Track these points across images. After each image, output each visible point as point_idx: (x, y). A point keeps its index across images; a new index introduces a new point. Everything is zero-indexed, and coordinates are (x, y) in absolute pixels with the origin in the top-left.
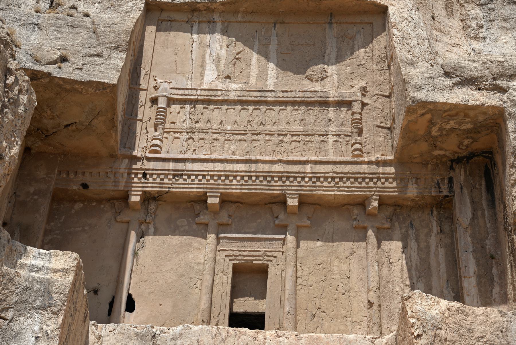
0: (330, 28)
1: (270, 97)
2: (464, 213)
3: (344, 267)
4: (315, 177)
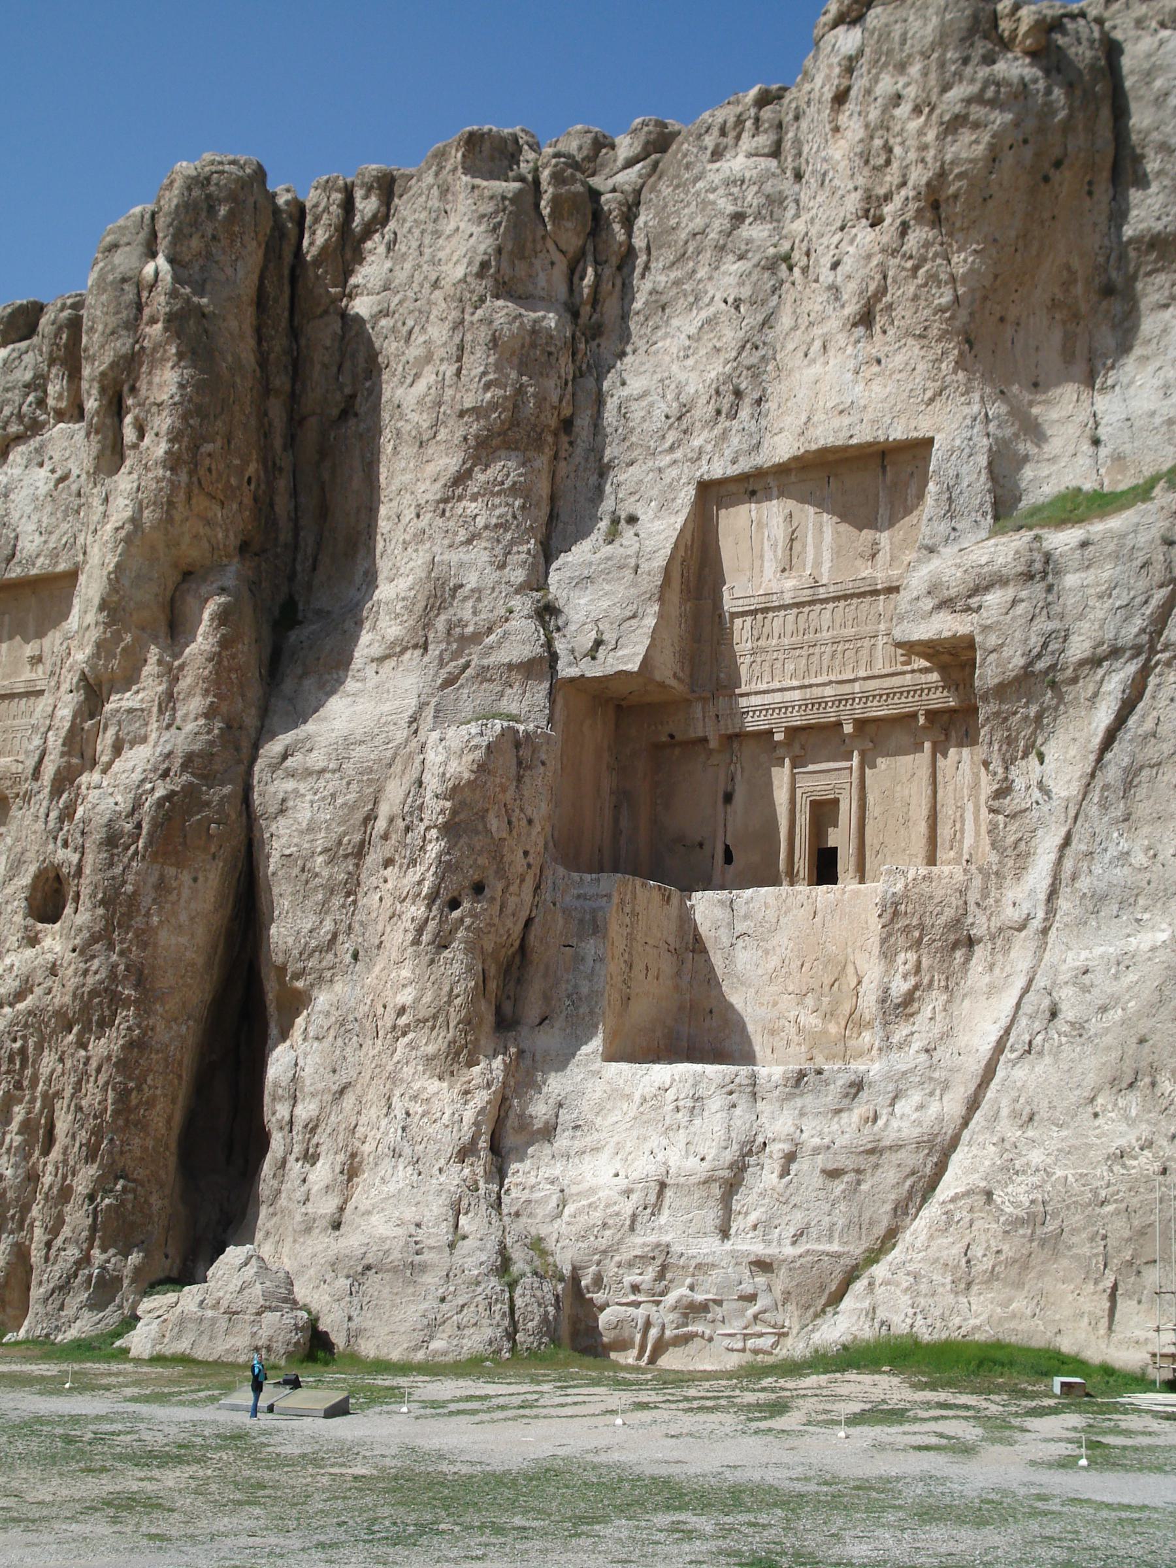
1: (822, 593)
3: (906, 792)
4: (867, 697)
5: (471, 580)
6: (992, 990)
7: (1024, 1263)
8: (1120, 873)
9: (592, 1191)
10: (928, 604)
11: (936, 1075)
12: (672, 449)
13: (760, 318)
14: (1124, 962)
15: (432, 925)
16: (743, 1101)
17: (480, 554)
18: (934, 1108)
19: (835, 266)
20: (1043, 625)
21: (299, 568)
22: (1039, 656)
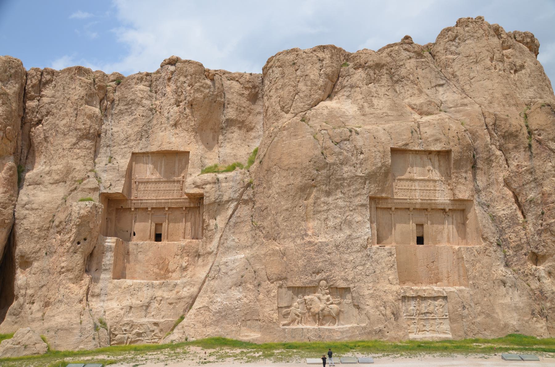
4: (171, 203)
5: (78, 168)
6: (204, 266)
7: (218, 321)
8: (233, 243)
9: (113, 309)
10: (193, 186)
12: (125, 144)
13: (148, 120)
14: (234, 261)
15: (73, 248)
17: (80, 162)
18: (192, 290)
19: (168, 113)
20: (218, 193)
21: (22, 158)
22: (217, 199)
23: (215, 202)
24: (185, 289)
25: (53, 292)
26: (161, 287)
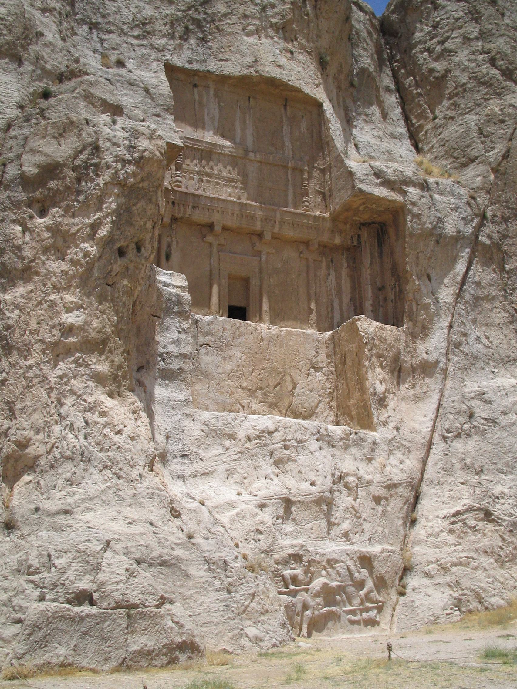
0: (285, 109)
2: (367, 260)
6: (417, 399)
11: (404, 443)
16: (325, 445)
23: (431, 233)
24: (393, 460)
25: (38, 418)
26: (346, 447)
